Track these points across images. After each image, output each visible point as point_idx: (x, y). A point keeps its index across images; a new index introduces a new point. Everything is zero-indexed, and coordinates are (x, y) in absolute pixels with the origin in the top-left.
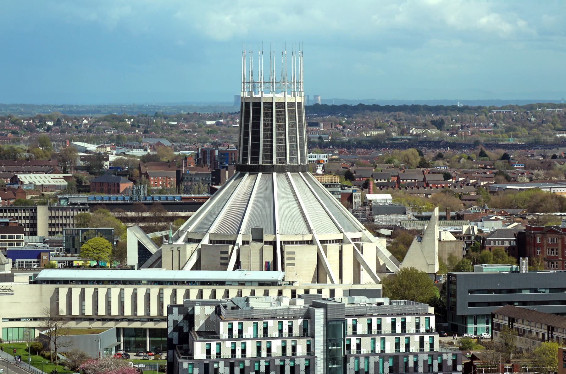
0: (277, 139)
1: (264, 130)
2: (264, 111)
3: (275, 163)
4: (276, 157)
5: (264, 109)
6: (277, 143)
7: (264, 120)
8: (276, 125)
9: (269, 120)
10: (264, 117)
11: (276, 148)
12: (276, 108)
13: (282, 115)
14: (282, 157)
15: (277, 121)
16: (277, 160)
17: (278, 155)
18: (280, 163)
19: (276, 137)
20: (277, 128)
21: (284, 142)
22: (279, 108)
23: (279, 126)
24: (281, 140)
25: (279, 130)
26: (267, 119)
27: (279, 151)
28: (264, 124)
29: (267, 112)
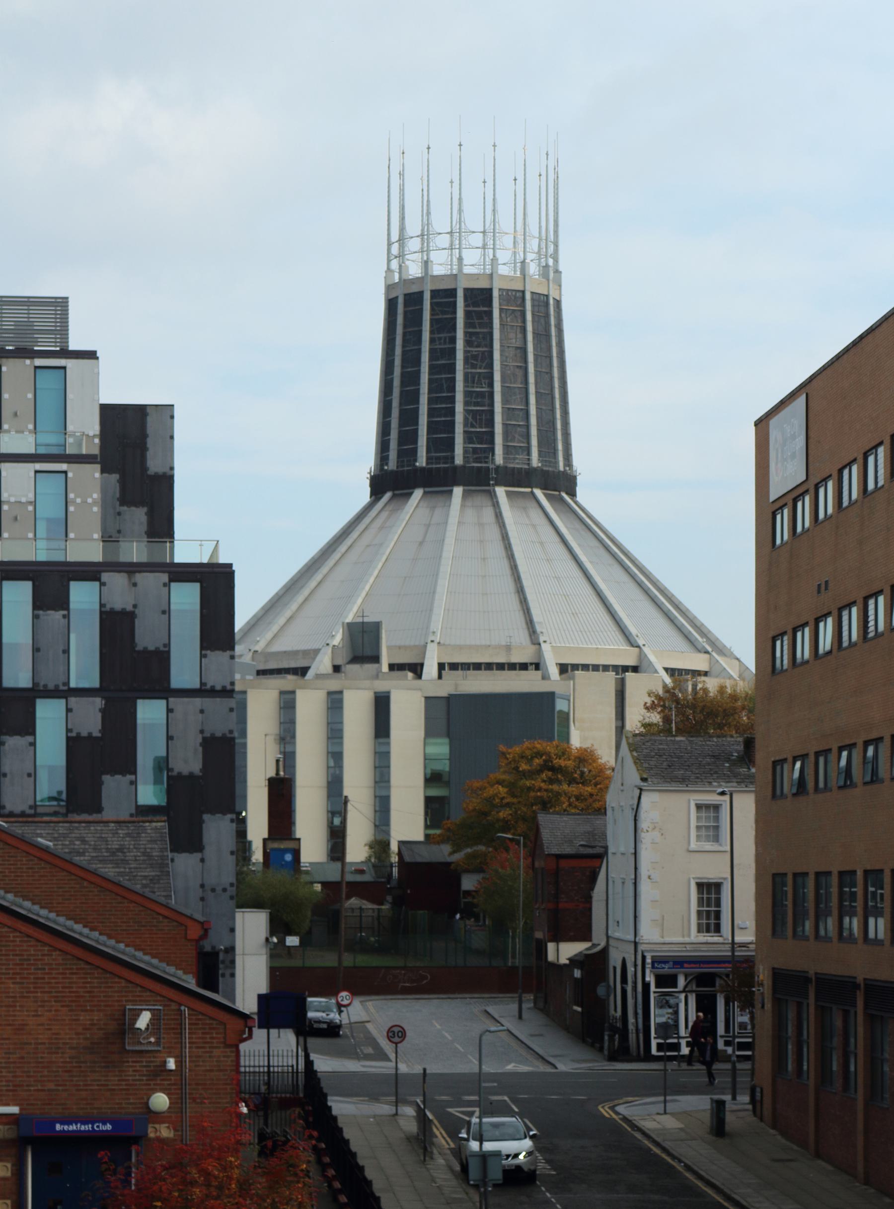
0: (467, 394)
1: (432, 368)
2: (432, 315)
3: (459, 460)
4: (465, 443)
5: (432, 309)
6: (466, 403)
7: (432, 341)
8: (465, 352)
9: (445, 338)
10: (432, 332)
11: (466, 419)
12: (466, 306)
13: (481, 325)
14: (481, 443)
15: (468, 342)
16: (465, 451)
17: (469, 437)
18: (477, 460)
19: (465, 386)
20: (466, 360)
21: (487, 401)
22: (475, 304)
23: (475, 357)
24: (481, 395)
25: (474, 366)
26: (440, 339)
27: (472, 426)
28: (432, 351)
29: (440, 316)
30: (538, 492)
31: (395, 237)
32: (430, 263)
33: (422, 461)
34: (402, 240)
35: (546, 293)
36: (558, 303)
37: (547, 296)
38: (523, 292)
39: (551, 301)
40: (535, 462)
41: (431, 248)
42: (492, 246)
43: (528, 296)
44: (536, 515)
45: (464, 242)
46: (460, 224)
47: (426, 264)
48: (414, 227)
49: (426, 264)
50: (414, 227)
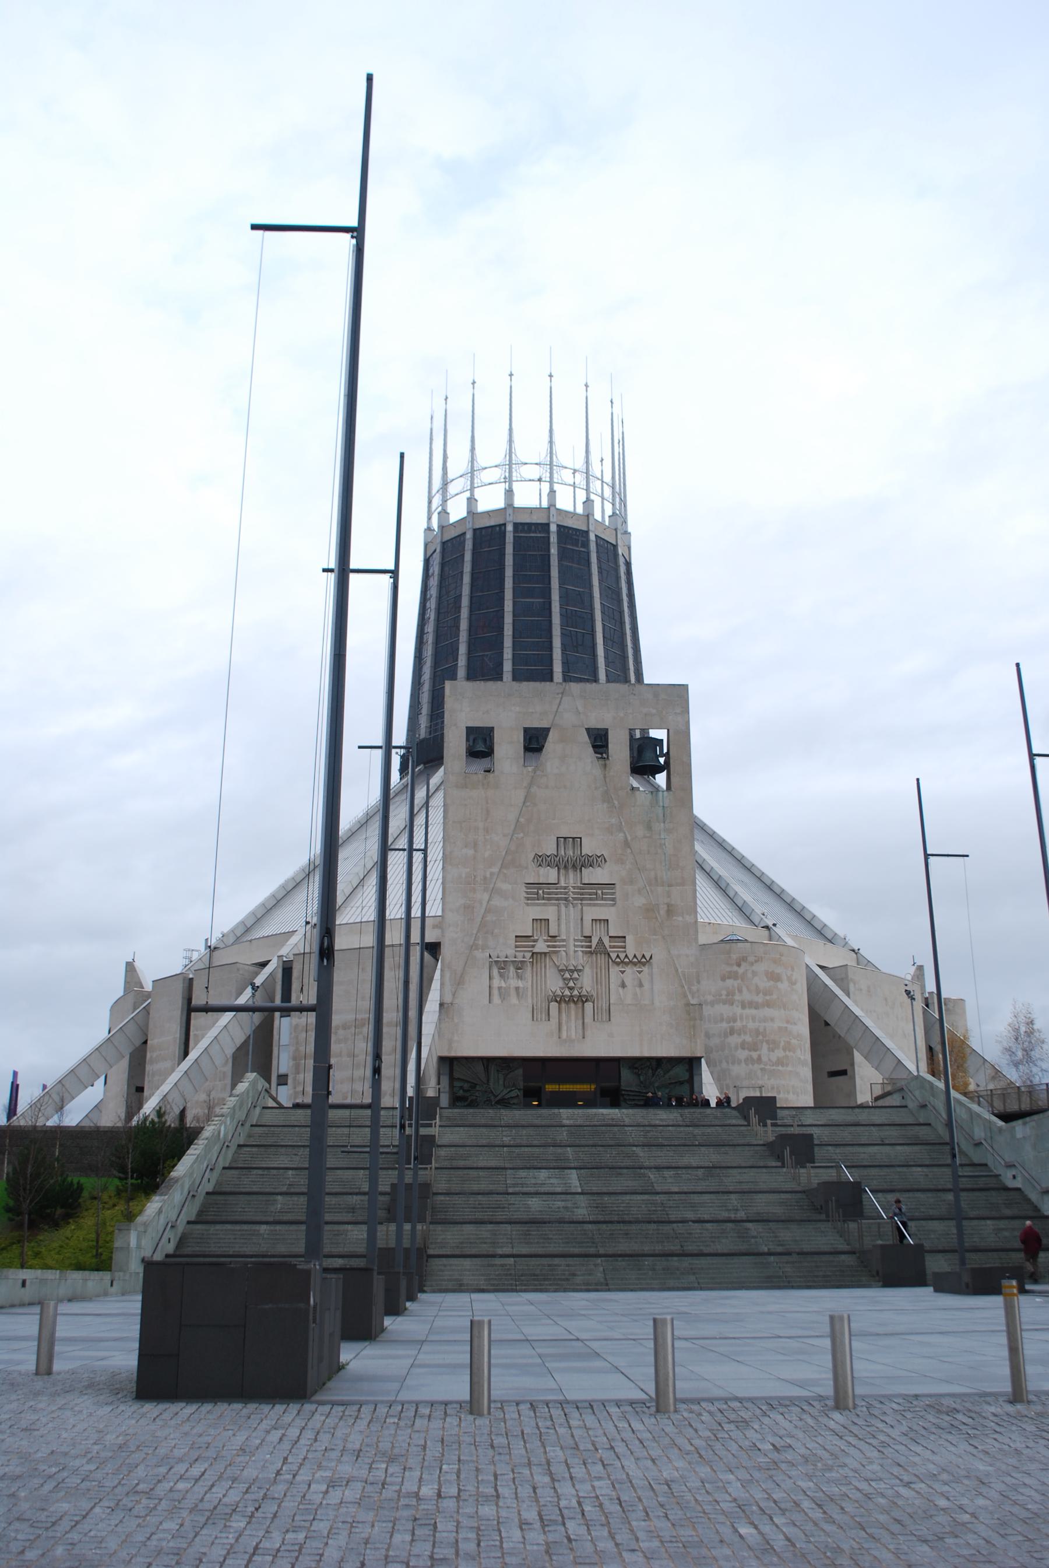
31: (437, 483)
32: (473, 500)
34: (445, 484)
35: (614, 543)
36: (628, 565)
37: (615, 547)
38: (587, 532)
39: (620, 553)
41: (476, 485)
42: (548, 479)
43: (592, 537)
45: (514, 474)
46: (510, 456)
47: (471, 501)
48: (458, 465)
49: (471, 501)
50: (458, 465)
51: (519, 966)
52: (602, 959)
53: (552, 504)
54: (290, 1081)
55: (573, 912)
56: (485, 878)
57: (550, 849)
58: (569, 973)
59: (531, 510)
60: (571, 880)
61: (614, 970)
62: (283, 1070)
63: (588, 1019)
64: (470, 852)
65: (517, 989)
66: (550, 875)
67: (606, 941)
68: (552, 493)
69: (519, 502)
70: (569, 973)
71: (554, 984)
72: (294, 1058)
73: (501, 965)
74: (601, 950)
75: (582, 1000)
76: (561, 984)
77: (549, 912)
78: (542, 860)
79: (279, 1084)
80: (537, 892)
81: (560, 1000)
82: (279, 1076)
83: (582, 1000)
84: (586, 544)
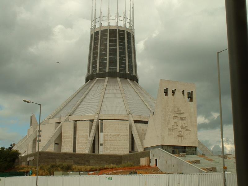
30: (128, 80)
33: (98, 71)
40: (127, 72)
44: (128, 86)
51: (173, 130)
52: (184, 129)
53: (117, 25)
54: (103, 145)
55: (180, 122)
56: (167, 115)
57: (176, 110)
58: (180, 132)
59: (113, 26)
60: (179, 116)
61: (186, 132)
62: (101, 143)
63: (183, 138)
64: (165, 110)
65: (173, 134)
66: (177, 115)
67: (185, 127)
68: (118, 23)
69: (111, 24)
70: (180, 132)
71: (178, 134)
72: (104, 141)
73: (170, 130)
74: (184, 128)
75: (182, 136)
76: (178, 133)
77: (177, 121)
78: (175, 112)
79: (101, 145)
80: (175, 118)
81: (178, 136)
82: (101, 144)
83: (182, 136)
84: (124, 34)
